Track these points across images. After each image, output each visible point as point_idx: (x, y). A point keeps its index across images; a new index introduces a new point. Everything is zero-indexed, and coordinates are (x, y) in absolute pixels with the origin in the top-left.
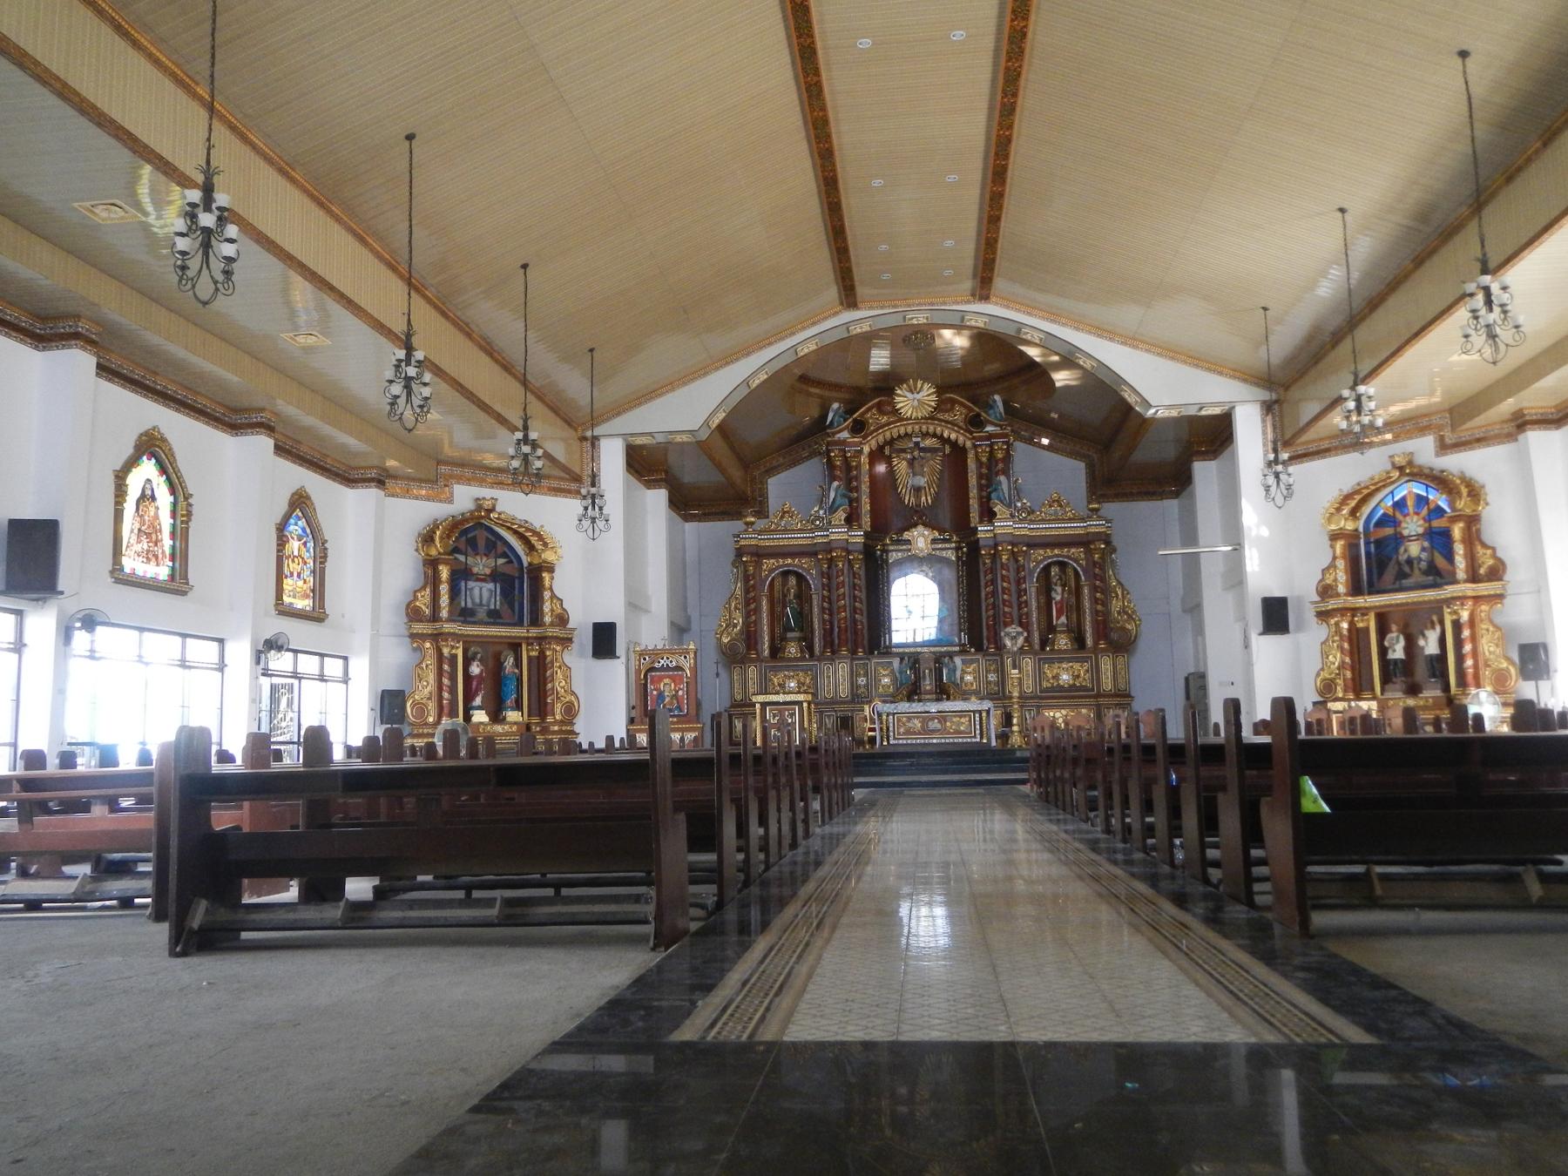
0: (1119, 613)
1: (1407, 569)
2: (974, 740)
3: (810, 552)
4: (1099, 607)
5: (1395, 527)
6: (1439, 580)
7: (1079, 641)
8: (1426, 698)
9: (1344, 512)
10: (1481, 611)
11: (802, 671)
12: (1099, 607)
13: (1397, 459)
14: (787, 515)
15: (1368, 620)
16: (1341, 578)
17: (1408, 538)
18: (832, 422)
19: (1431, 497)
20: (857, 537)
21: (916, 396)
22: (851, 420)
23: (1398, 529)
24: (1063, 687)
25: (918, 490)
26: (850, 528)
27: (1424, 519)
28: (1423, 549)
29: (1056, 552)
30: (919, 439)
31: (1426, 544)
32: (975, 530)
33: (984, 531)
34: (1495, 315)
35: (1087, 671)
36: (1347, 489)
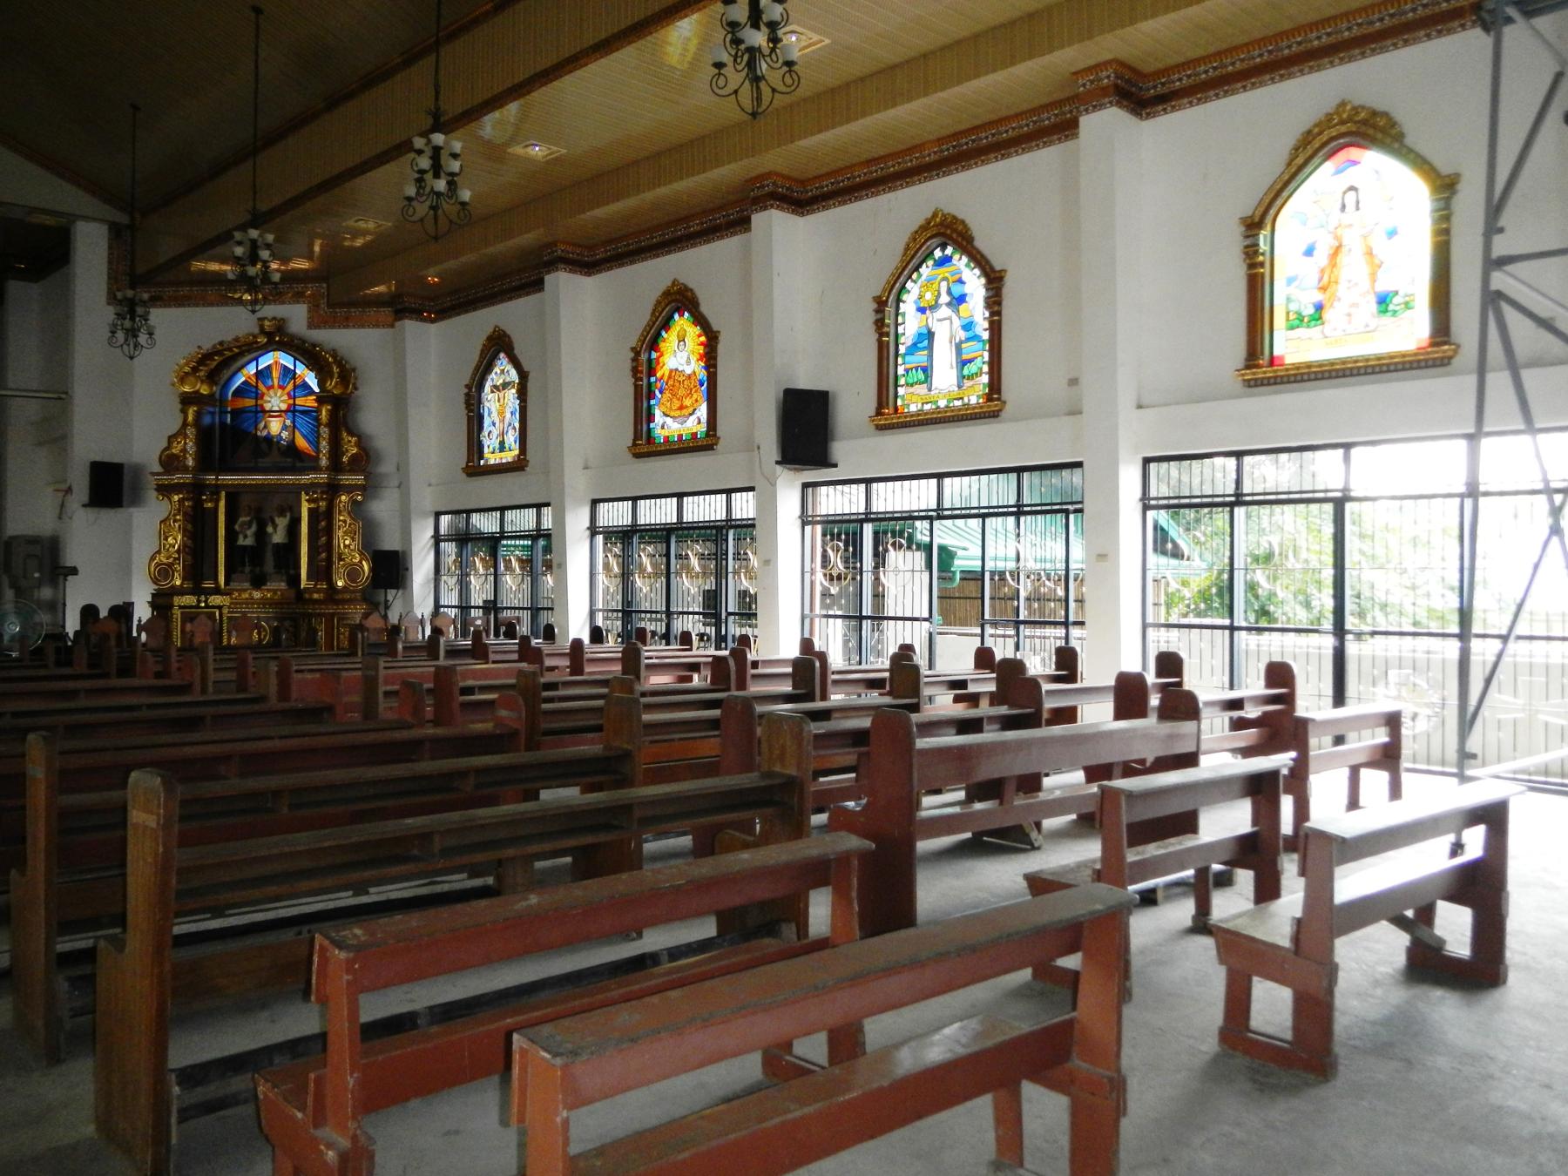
1: (264, 446)
5: (257, 399)
6: (299, 464)
8: (275, 592)
9: (202, 374)
10: (340, 502)
13: (267, 323)
15: (217, 502)
16: (188, 447)
17: (270, 413)
19: (298, 372)
23: (260, 402)
27: (289, 394)
28: (285, 428)
31: (288, 422)
34: (441, 185)
36: (207, 346)
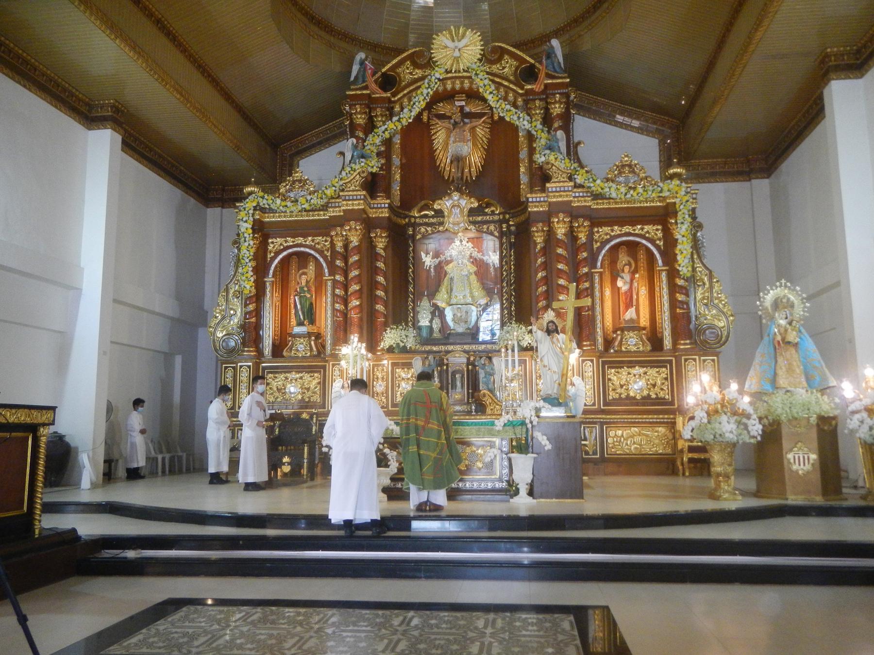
0: (706, 305)
2: (498, 485)
3: (324, 228)
4: (680, 297)
7: (656, 343)
11: (308, 372)
12: (680, 297)
14: (297, 185)
18: (356, 78)
20: (381, 208)
21: (456, 43)
22: (380, 74)
24: (634, 398)
25: (458, 160)
26: (373, 196)
29: (627, 229)
30: (463, 103)
32: (524, 205)
33: (536, 203)
35: (666, 379)
